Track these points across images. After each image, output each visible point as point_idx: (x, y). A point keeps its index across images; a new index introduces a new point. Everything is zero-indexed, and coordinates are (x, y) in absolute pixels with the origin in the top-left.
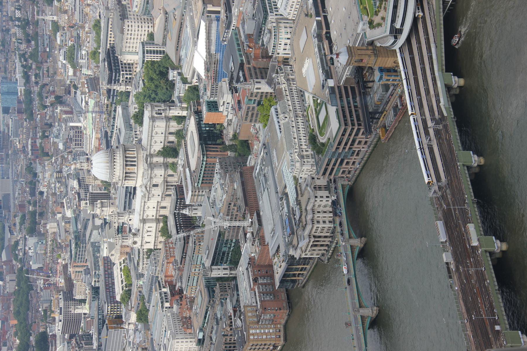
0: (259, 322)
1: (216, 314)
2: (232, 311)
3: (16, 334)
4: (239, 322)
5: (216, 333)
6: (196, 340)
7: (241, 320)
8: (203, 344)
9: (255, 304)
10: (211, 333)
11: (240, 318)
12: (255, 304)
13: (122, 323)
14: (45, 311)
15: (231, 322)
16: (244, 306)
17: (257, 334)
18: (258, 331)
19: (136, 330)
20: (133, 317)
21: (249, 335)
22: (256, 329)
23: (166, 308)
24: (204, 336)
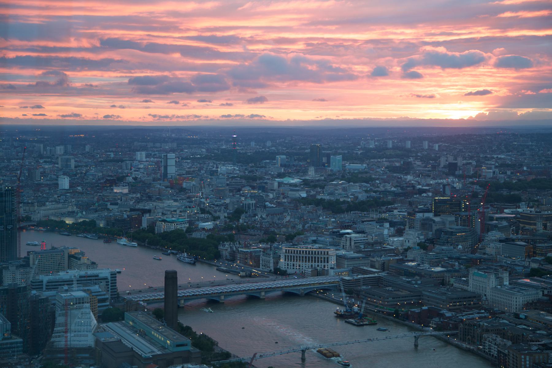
0: (536, 364)
1: (540, 330)
2: (543, 342)
3: (520, 180)
4: (535, 348)
5: (524, 328)
6: (519, 313)
7: (537, 350)
8: (516, 317)
9: (549, 362)
10: (524, 325)
11: (538, 349)
12: (549, 362)
13: (529, 256)
14: (537, 201)
15: (533, 342)
16: (548, 354)
17: (525, 362)
18: (528, 362)
19: (524, 267)
20: (535, 266)
21: (525, 355)
22: (529, 361)
23: (543, 291)
24: (521, 318)
